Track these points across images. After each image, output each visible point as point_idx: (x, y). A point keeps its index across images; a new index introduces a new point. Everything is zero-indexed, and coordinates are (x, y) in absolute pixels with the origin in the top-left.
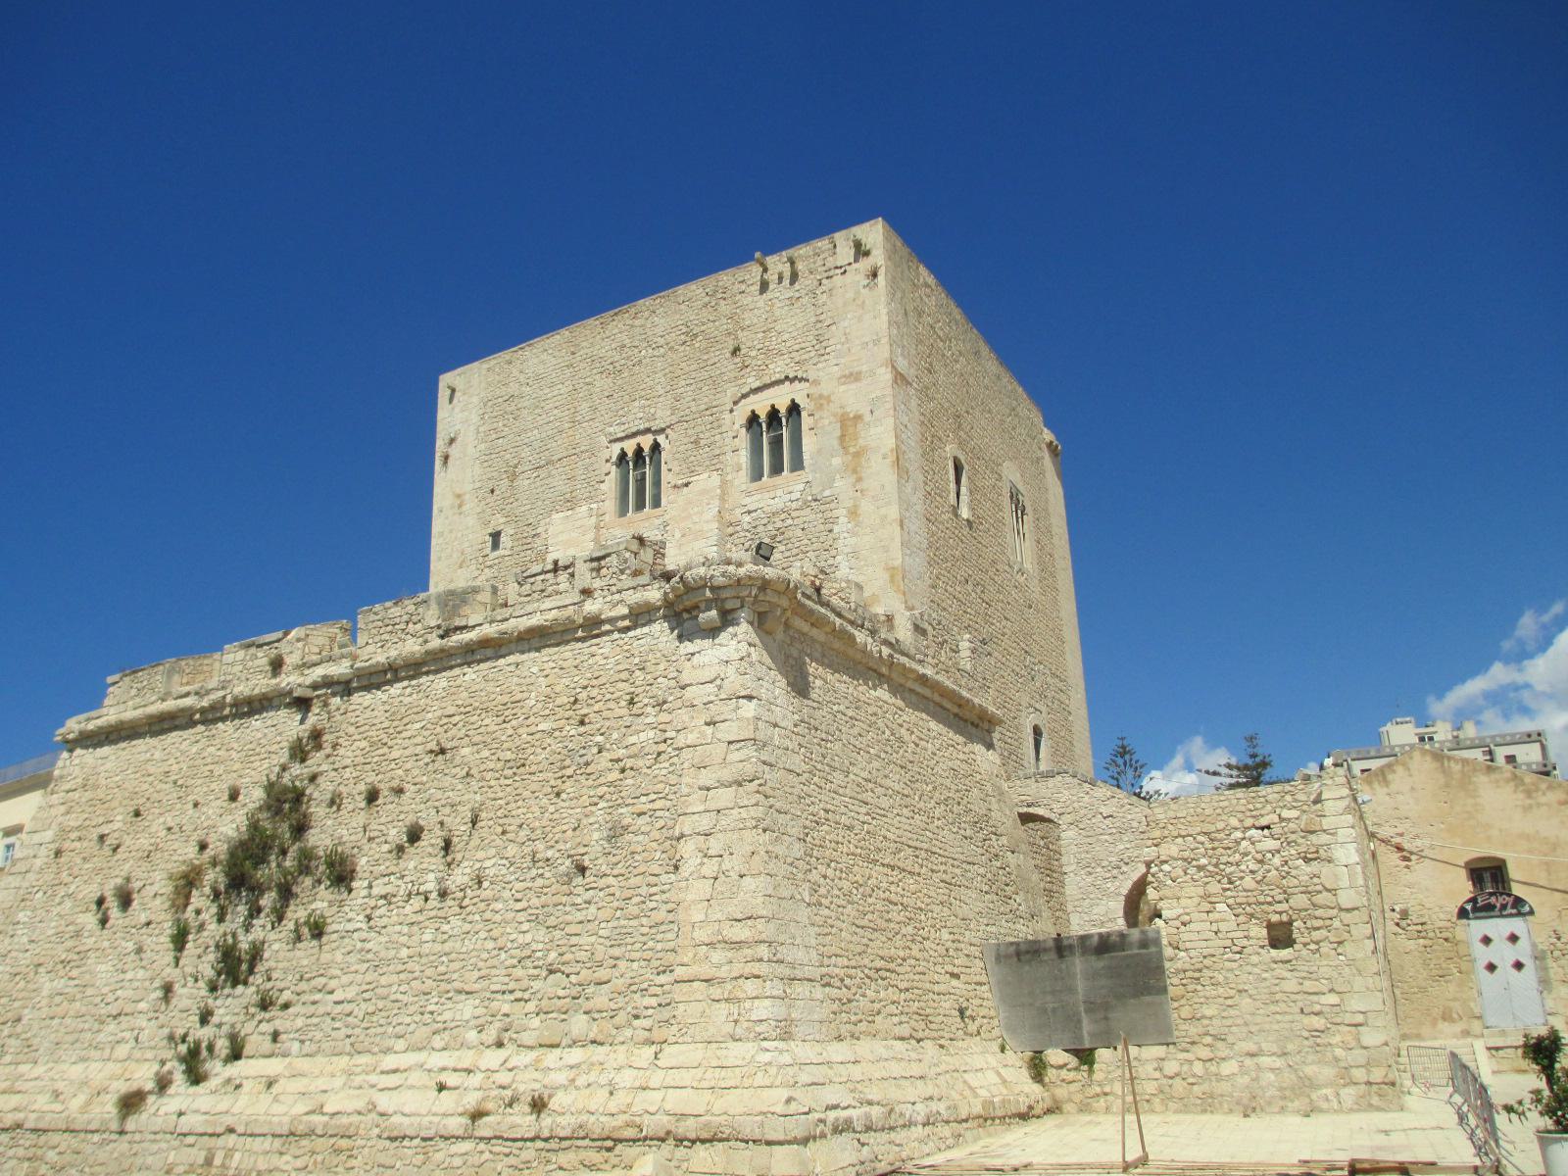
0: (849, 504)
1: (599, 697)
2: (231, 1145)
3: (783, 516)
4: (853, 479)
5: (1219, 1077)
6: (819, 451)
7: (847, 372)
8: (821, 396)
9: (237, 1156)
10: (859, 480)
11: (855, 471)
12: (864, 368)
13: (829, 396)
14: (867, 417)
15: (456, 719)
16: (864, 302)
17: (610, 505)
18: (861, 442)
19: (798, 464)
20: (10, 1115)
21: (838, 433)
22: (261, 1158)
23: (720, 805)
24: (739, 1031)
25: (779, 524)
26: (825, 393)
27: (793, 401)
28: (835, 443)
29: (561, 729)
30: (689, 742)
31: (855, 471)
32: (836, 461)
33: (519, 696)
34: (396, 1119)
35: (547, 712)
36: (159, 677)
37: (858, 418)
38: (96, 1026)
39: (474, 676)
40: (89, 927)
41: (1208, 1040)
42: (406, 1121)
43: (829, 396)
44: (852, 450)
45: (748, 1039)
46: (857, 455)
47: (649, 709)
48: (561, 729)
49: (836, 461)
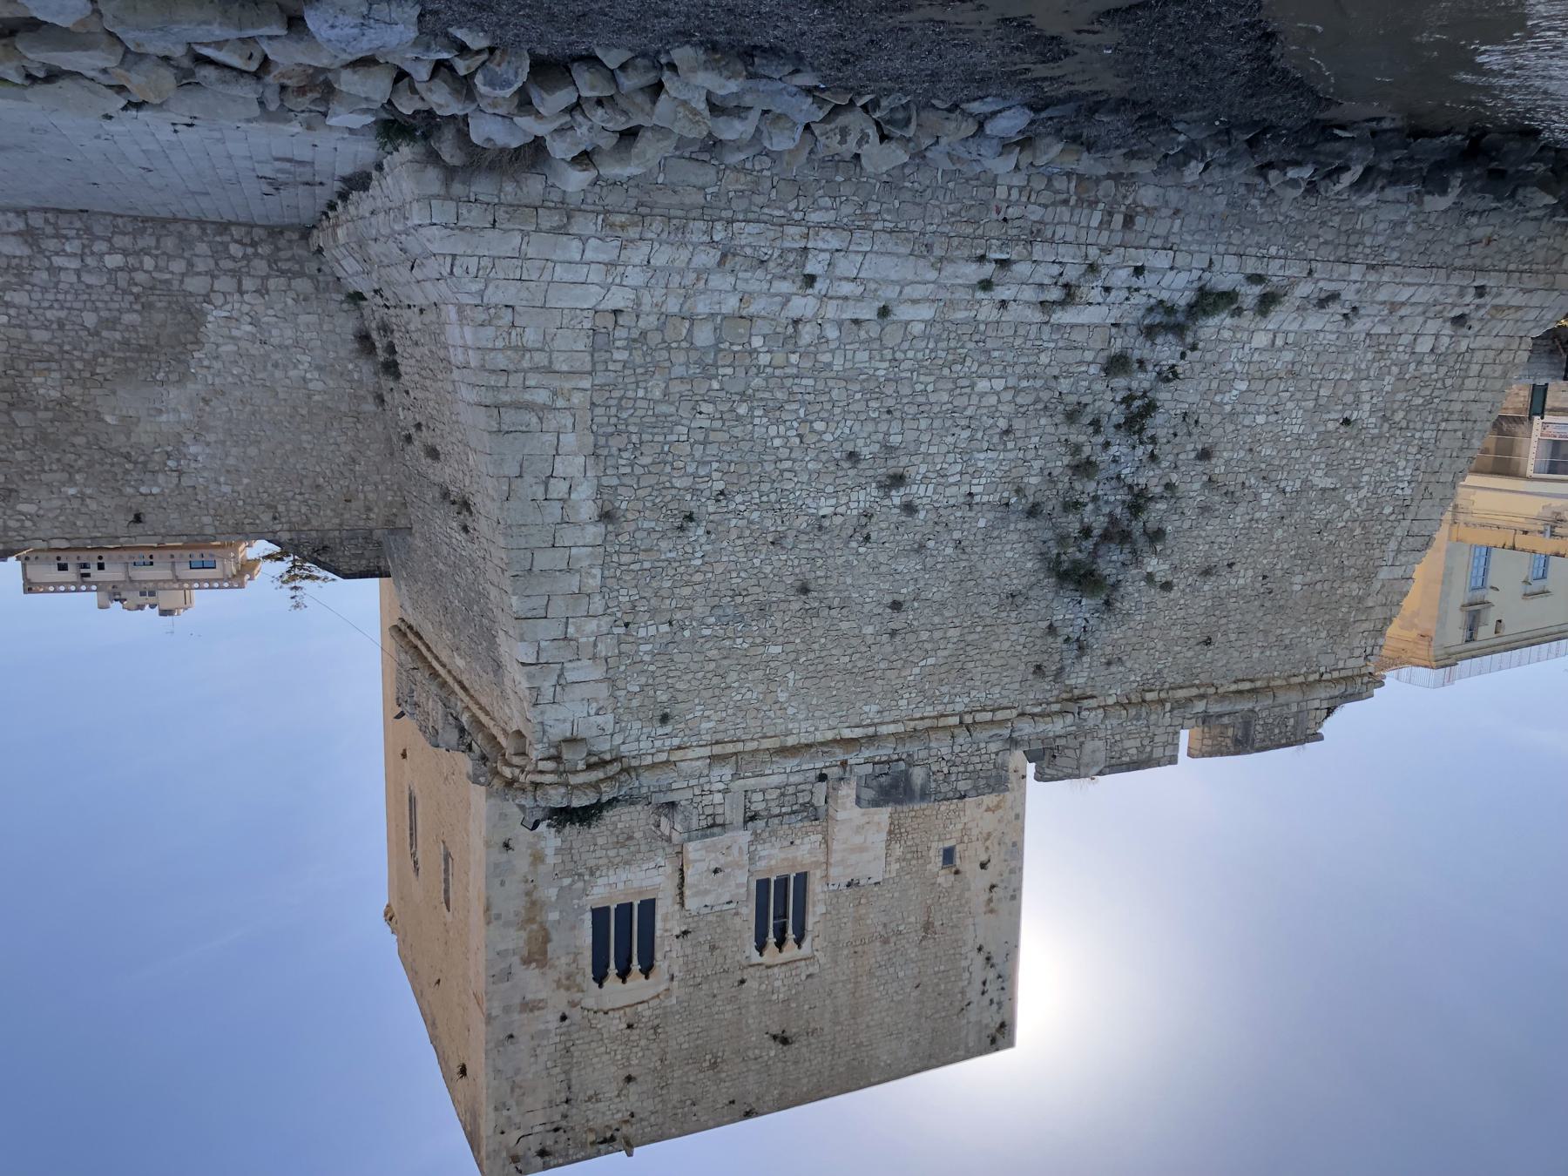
0: (542, 868)
1: (709, 675)
2: (1105, 234)
3: (618, 860)
4: (535, 896)
5: (125, 253)
6: (573, 928)
7: (537, 1013)
8: (568, 989)
9: (1095, 223)
10: (528, 894)
11: (533, 903)
12: (516, 1016)
13: (558, 987)
14: (516, 960)
15: (883, 665)
16: (512, 1090)
17: (816, 888)
18: (524, 934)
19: (600, 915)
20: (1385, 279)
21: (549, 946)
22: (1066, 219)
23: (551, 552)
24: (507, 316)
25: (623, 851)
26: (562, 991)
27: (601, 986)
28: (554, 936)
29: (753, 645)
30: (595, 622)
31: (533, 903)
32: (554, 916)
33: (808, 683)
34: (904, 250)
35: (772, 664)
36: (1259, 736)
37: (526, 962)
38: (1297, 368)
39: (866, 709)
40: (1320, 473)
41: (135, 290)
42: (890, 247)
43: (558, 987)
44: (535, 927)
45: (496, 306)
46: (531, 920)
47: (647, 658)
48: (753, 645)
49: (554, 916)
